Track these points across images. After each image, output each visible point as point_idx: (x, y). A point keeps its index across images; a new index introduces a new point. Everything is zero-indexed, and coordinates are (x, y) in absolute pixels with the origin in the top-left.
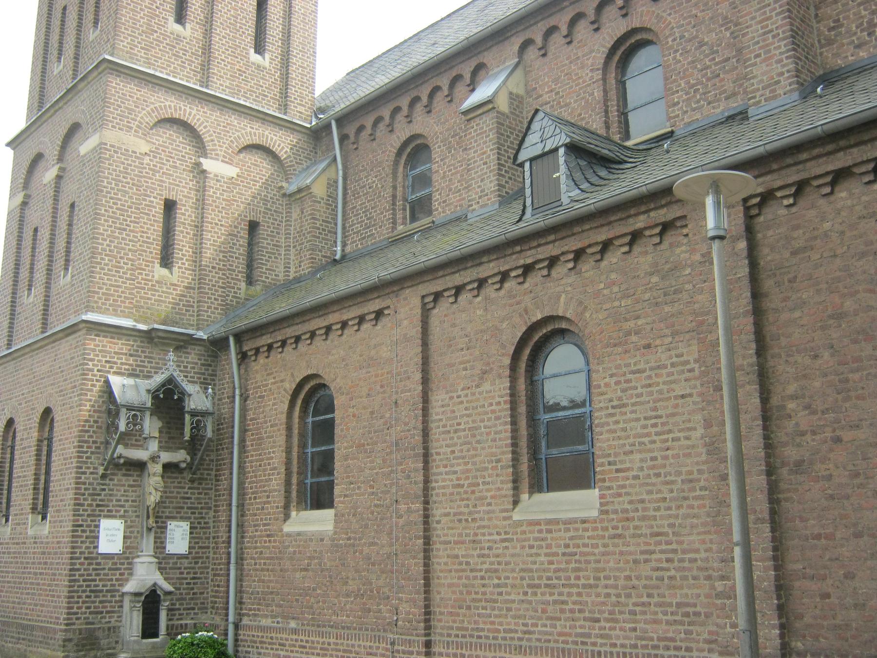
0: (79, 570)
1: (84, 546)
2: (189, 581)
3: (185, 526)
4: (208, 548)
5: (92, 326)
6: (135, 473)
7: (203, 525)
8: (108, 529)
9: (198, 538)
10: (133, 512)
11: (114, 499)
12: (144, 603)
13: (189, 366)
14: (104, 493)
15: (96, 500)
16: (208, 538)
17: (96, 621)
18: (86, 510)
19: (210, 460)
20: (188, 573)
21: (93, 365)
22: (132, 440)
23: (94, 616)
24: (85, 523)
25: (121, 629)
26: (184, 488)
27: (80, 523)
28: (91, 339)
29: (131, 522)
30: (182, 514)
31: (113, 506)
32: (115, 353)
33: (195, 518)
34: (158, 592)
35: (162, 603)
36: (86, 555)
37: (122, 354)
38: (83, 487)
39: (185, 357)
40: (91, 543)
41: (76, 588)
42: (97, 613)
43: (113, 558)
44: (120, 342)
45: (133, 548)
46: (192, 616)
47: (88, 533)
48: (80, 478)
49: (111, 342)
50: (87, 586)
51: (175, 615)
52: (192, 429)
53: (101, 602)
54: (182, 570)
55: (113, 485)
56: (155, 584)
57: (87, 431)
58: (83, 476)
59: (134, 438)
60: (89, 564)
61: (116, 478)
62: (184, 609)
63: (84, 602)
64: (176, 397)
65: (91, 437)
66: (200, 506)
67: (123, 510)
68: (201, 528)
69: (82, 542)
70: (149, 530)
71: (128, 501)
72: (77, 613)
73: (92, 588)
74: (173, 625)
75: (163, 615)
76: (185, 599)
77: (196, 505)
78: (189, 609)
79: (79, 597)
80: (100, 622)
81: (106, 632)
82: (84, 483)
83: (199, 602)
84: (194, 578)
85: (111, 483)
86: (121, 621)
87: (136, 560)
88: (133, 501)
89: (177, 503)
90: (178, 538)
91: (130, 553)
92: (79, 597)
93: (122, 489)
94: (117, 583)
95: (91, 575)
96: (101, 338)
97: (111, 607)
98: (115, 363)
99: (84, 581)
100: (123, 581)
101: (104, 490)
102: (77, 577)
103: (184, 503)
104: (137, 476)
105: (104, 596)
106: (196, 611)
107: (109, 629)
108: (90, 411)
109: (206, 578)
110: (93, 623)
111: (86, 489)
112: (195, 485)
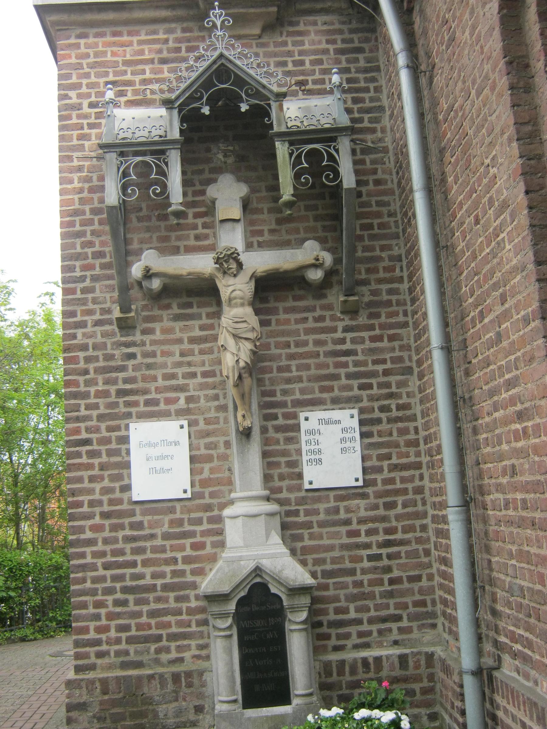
0: (91, 542)
1: (97, 486)
2: (375, 551)
3: (348, 419)
4: (418, 466)
5: (64, 17)
6: (204, 311)
7: (395, 413)
8: (150, 445)
9: (387, 445)
10: (208, 398)
11: (159, 373)
12: (238, 616)
13: (307, 60)
14: (130, 363)
15: (114, 382)
16: (415, 443)
17: (145, 658)
18: (96, 406)
19: (391, 258)
20: (369, 533)
21: (79, 96)
22: (187, 238)
23: (140, 647)
24: (94, 436)
25: (206, 676)
26: (334, 330)
27: (84, 435)
28: (69, 46)
29: (207, 422)
30: (336, 393)
31: (158, 390)
32: (127, 63)
33: (371, 398)
34: (273, 590)
35: (290, 616)
36: (106, 508)
37: (142, 62)
38: (81, 354)
39: (294, 44)
40: (113, 478)
41: (88, 585)
42: (147, 640)
43: (172, 510)
44: (135, 39)
45: (219, 482)
46: (395, 635)
47: (104, 458)
48: (74, 337)
49: (114, 44)
50: (115, 578)
51: (347, 636)
52: (297, 176)
53: (152, 614)
54: (354, 526)
55: (154, 343)
56: (258, 571)
57: (82, 234)
58: (79, 332)
59: (192, 233)
60: (115, 528)
61: (157, 326)
62: (371, 621)
63: (111, 616)
64: (244, 107)
65: (91, 244)
66: (380, 368)
67: (182, 396)
68: (389, 421)
69: (92, 479)
70: (246, 434)
71: (193, 375)
72: (98, 642)
73: (129, 583)
74: (342, 663)
75: (297, 646)
76: (371, 596)
77: (371, 367)
78: (384, 620)
79: (99, 605)
80: (157, 661)
81: (170, 687)
82: (84, 347)
83: (408, 600)
84: (388, 544)
85: (147, 338)
86: (208, 658)
87: (227, 512)
88: (205, 374)
89: (319, 366)
90: (332, 450)
91: (212, 495)
92: (99, 605)
93: (176, 349)
94: (187, 568)
95: (121, 552)
96: (91, 40)
97: (180, 624)
98: (130, 83)
99: (107, 566)
100: (201, 563)
101: (132, 356)
102: (89, 560)
103: (338, 365)
104: (208, 316)
105: (158, 600)
106: (405, 623)
107: (176, 678)
108: (81, 191)
109: (419, 540)
110: (139, 665)
111: (88, 360)
112: (362, 319)
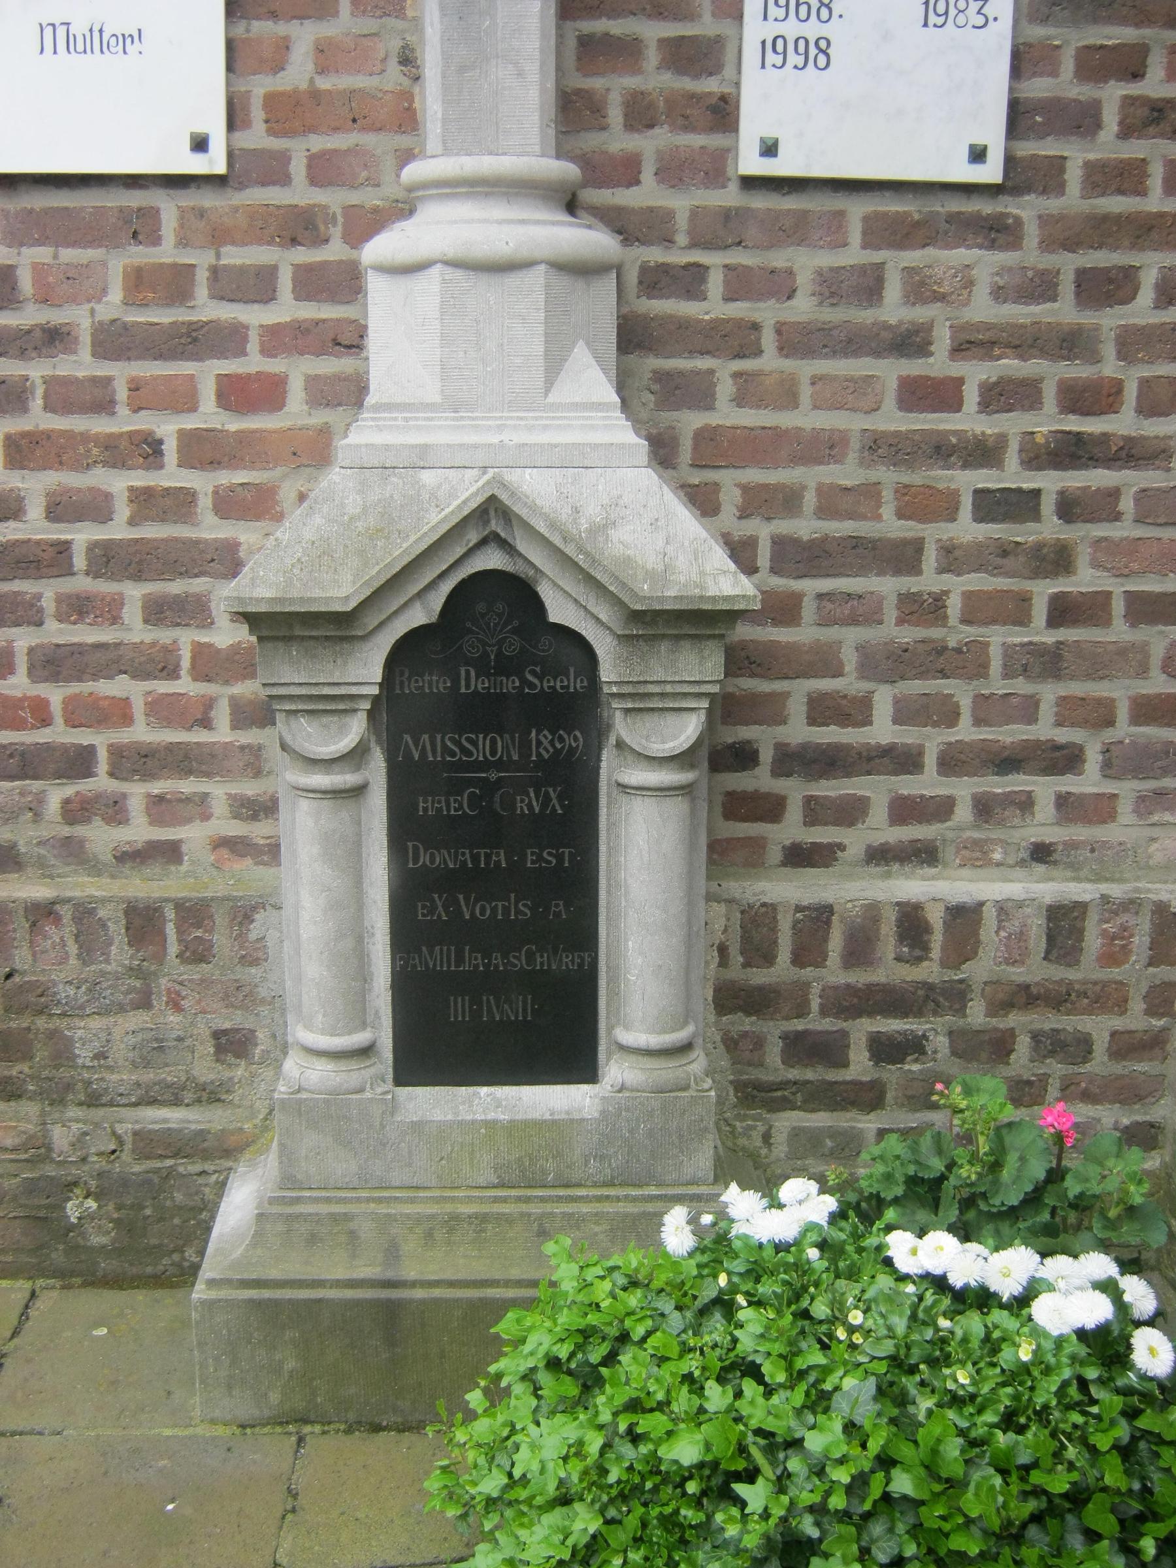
2: (1012, 475)
12: (392, 710)
20: (997, 397)
34: (559, 611)
35: (622, 727)
43: (142, 228)
45: (356, 114)
46: (1043, 825)
51: (850, 812)
54: (939, 363)
56: (492, 517)
62: (953, 762)
80: (73, 851)
81: (120, 953)
83: (1119, 692)
84: (1071, 452)
86: (271, 852)
87: (382, 247)
91: (323, 170)
97: (164, 711)
100: (262, 464)
105: (77, 608)
106: (1088, 781)
107: (143, 922)
